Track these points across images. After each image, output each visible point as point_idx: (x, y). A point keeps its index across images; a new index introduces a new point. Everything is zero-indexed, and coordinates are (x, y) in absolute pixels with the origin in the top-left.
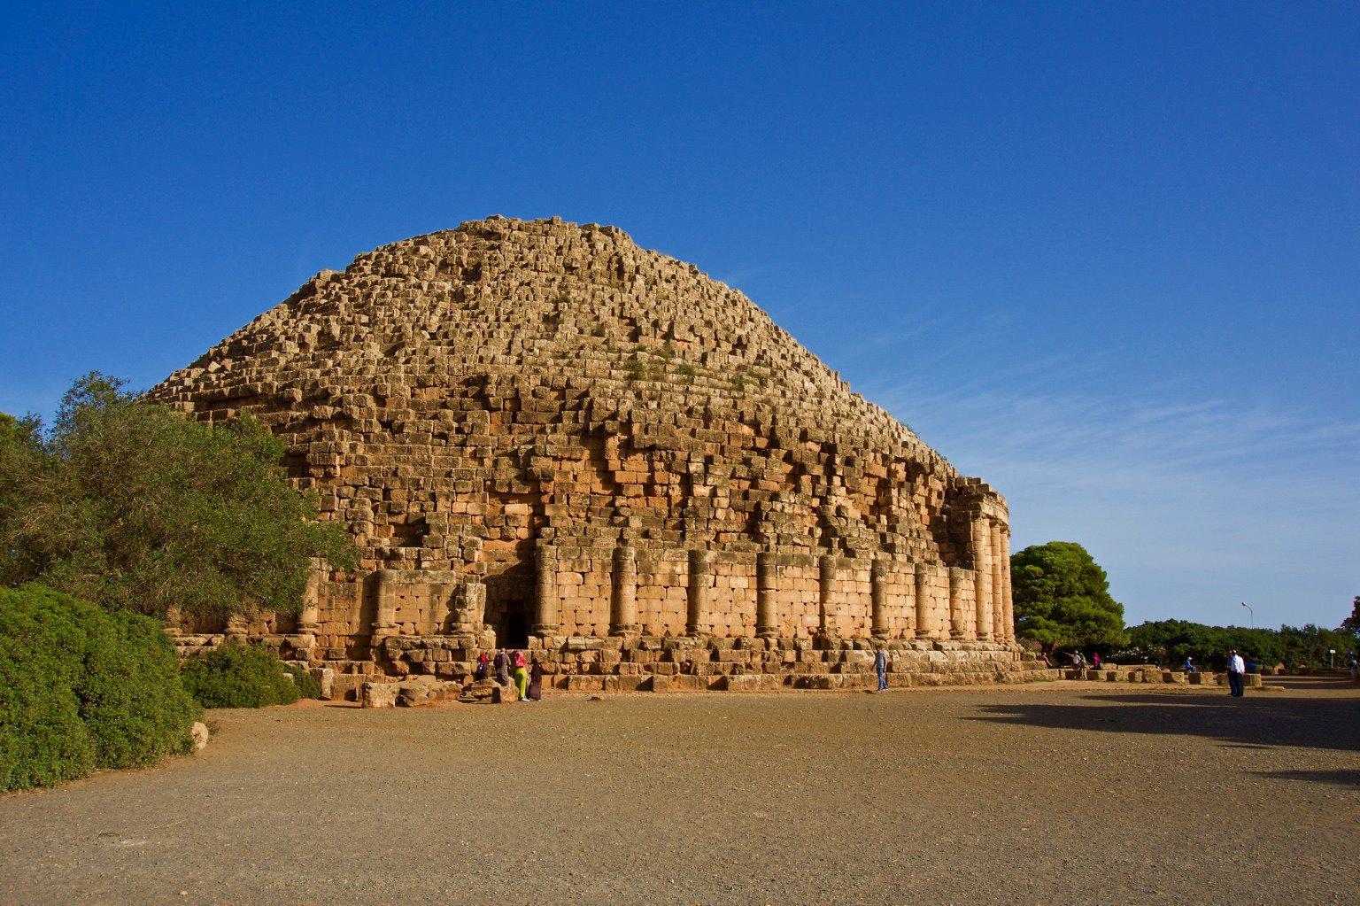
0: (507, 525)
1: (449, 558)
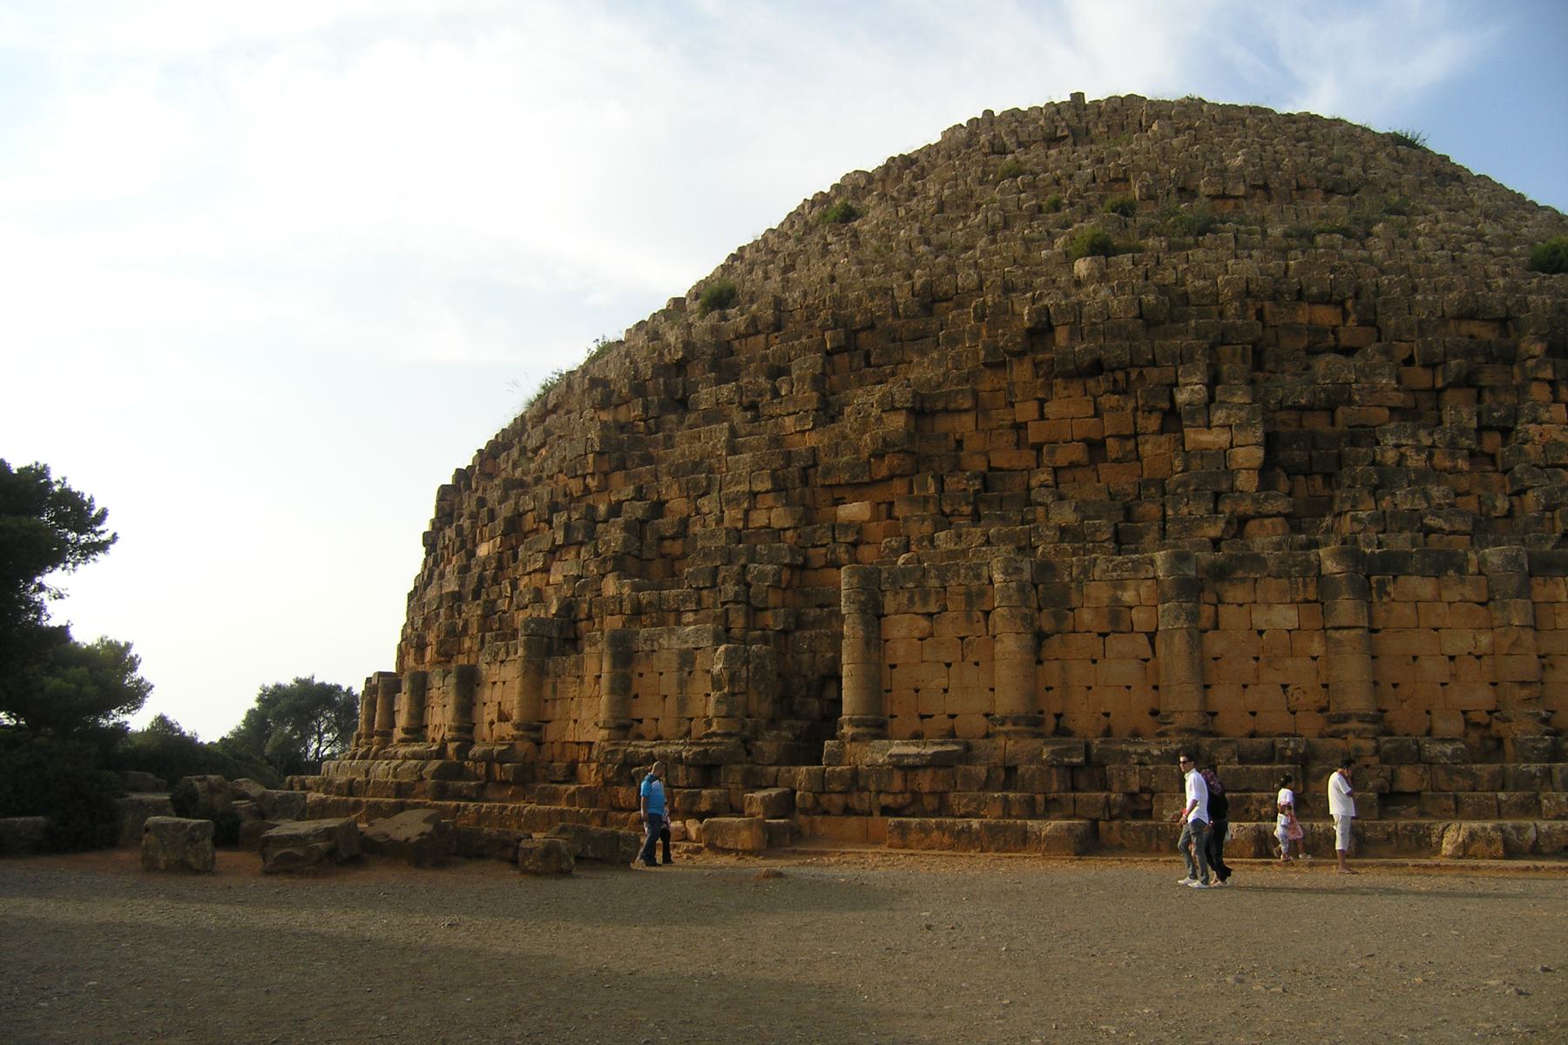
0: (834, 540)
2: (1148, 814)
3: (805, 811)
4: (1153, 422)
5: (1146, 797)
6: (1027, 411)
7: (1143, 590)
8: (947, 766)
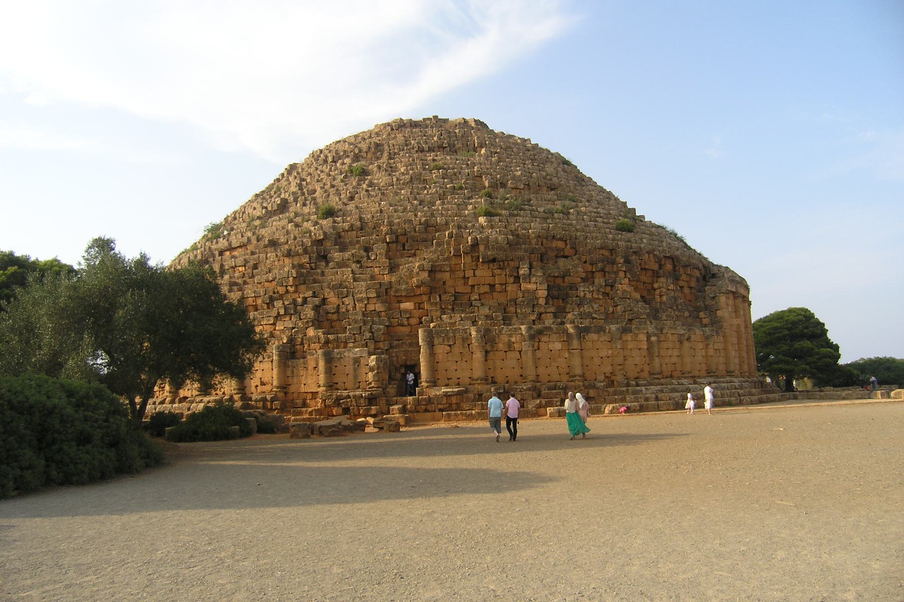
3: (411, 412)
4: (512, 280)
6: (469, 273)
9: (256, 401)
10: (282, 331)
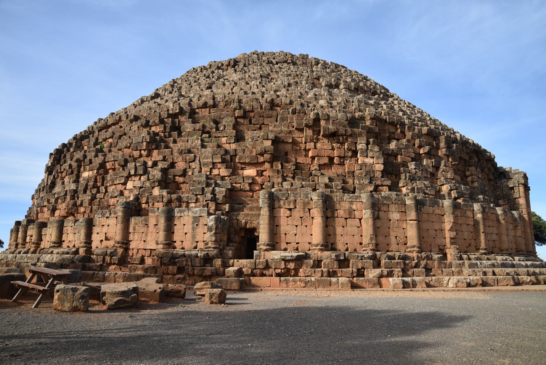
0: (244, 182)
1: (206, 201)
2: (363, 276)
4: (350, 154)
5: (363, 270)
7: (358, 205)
8: (299, 260)
9: (97, 255)
10: (131, 191)
